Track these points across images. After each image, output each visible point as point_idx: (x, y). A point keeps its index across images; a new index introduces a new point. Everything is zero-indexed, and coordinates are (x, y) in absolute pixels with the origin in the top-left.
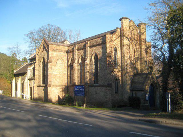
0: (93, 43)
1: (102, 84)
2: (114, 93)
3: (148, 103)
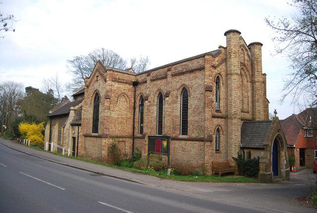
0: (180, 69)
1: (194, 135)
2: (214, 151)
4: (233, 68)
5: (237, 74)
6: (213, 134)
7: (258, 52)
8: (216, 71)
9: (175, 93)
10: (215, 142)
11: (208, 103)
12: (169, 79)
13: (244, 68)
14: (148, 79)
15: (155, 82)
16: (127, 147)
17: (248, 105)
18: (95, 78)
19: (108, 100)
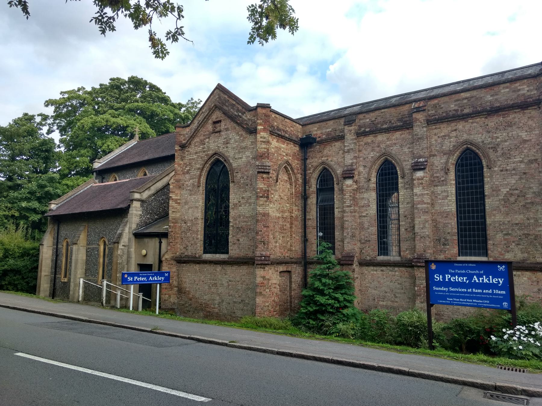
0: (453, 106)
9: (438, 162)
12: (419, 130)
14: (350, 133)
16: (293, 286)
18: (209, 127)
19: (265, 176)
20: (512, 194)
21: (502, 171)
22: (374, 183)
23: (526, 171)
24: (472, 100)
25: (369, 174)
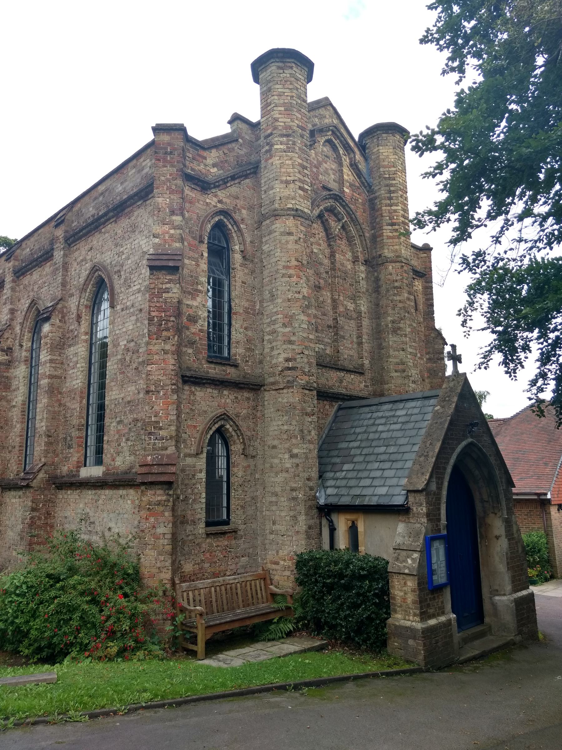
2: (201, 528)
3: (449, 606)
4: (279, 190)
5: (297, 214)
6: (193, 450)
7: (392, 158)
8: (212, 200)
10: (201, 488)
11: (161, 319)
13: (340, 209)
15: (26, 280)
17: (360, 344)
20: (128, 350)
21: (122, 310)
22: (26, 351)
23: (142, 306)
24: (107, 194)
25: (22, 335)
